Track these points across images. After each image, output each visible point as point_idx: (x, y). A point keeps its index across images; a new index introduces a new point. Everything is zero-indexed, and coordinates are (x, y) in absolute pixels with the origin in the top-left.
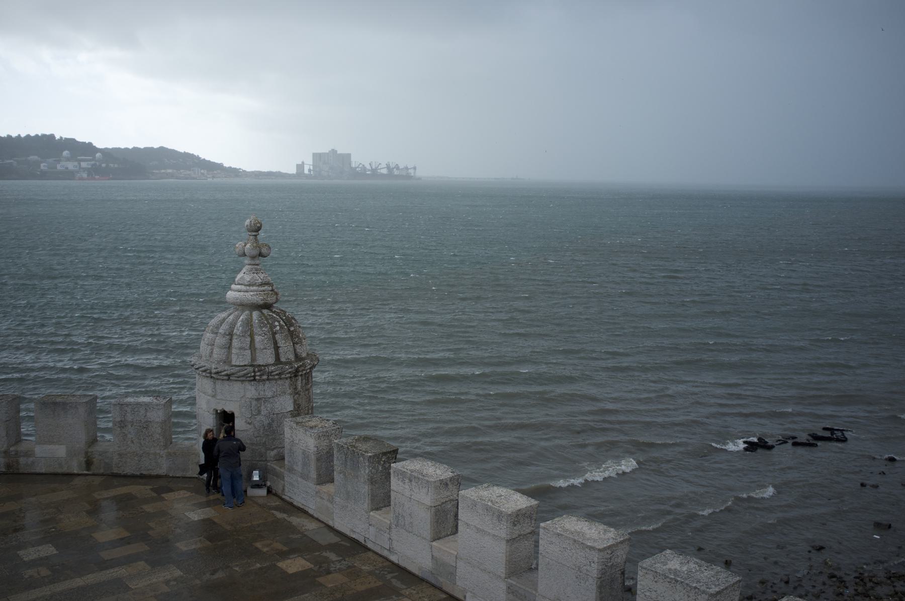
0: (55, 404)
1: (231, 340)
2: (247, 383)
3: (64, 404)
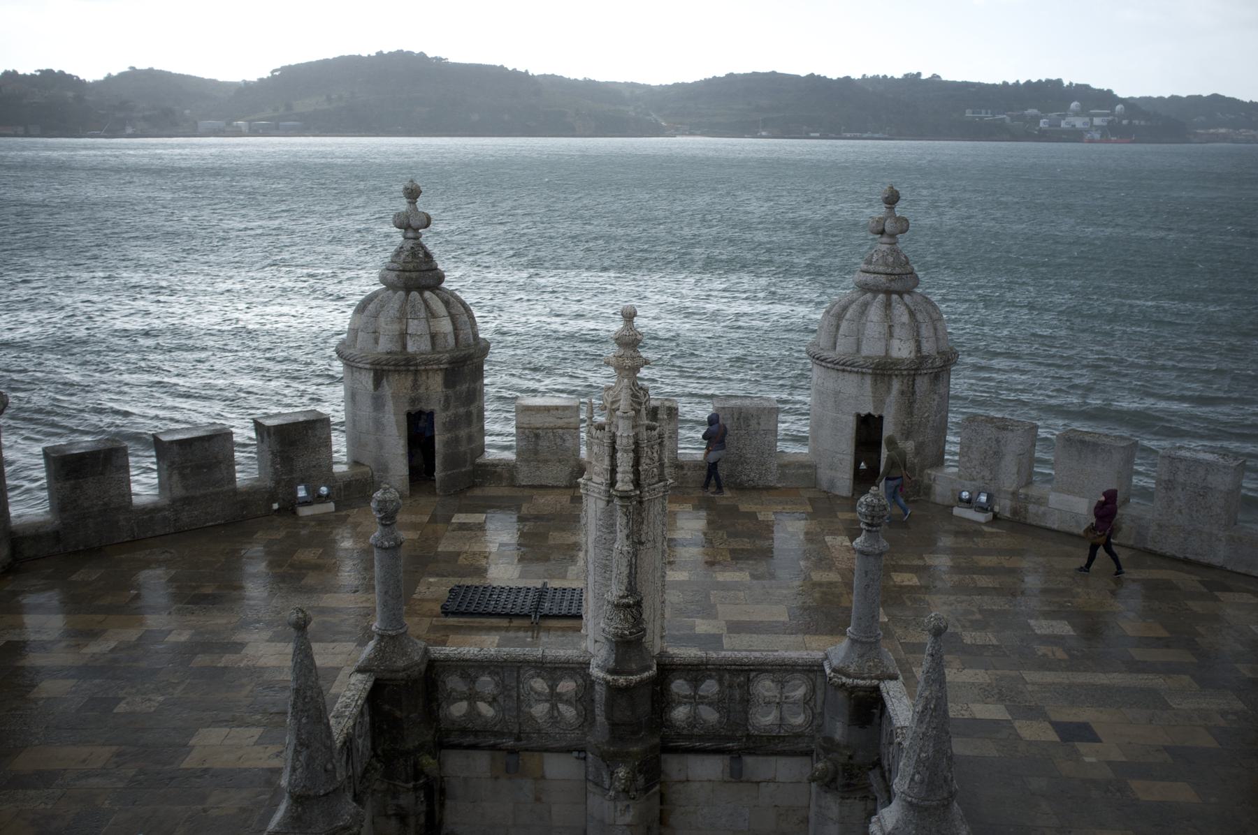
0: (1083, 442)
3: (1095, 444)
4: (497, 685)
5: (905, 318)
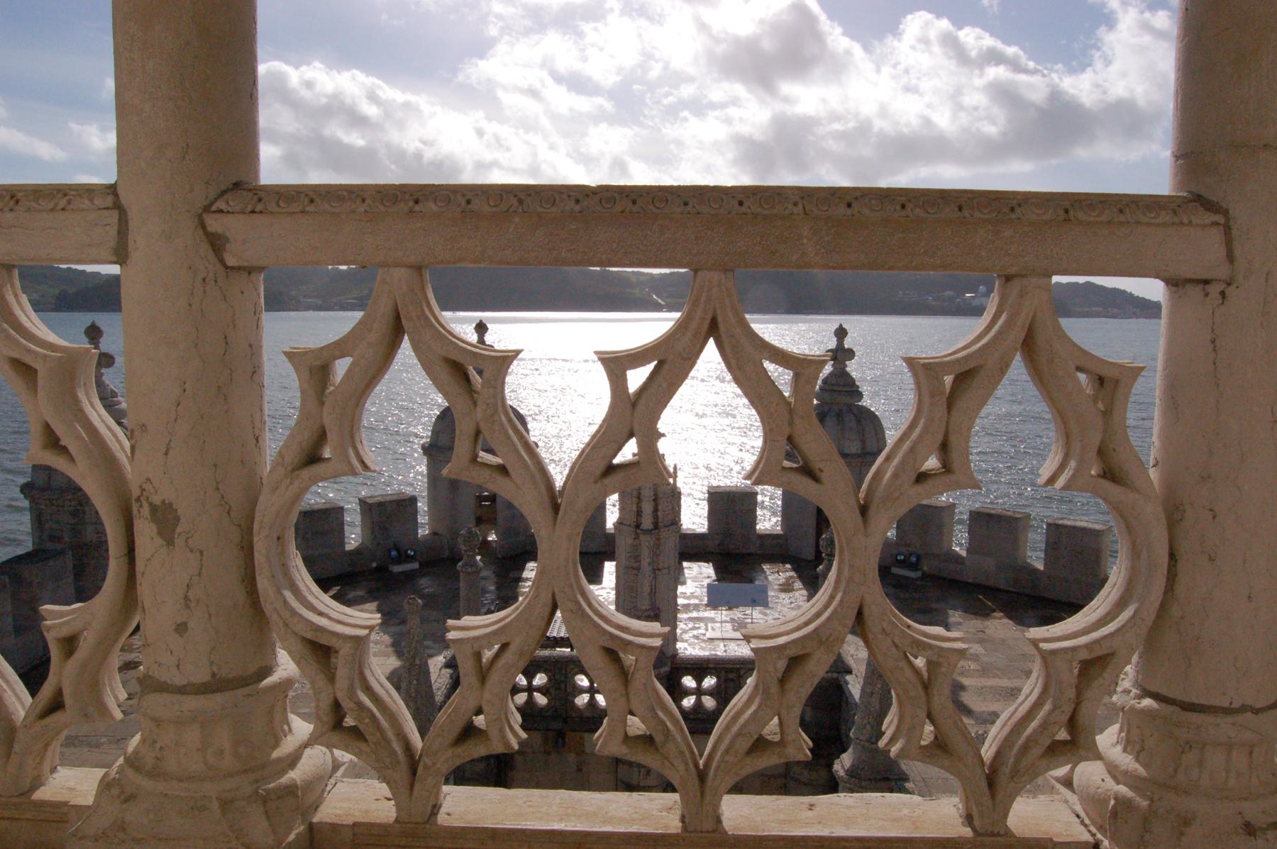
4: (550, 680)
5: (853, 424)
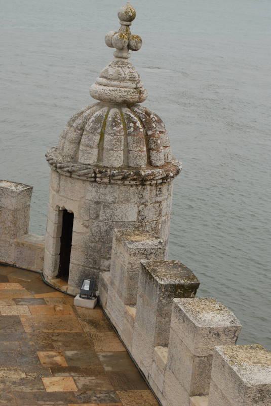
1: (82, 135)
2: (88, 184)
